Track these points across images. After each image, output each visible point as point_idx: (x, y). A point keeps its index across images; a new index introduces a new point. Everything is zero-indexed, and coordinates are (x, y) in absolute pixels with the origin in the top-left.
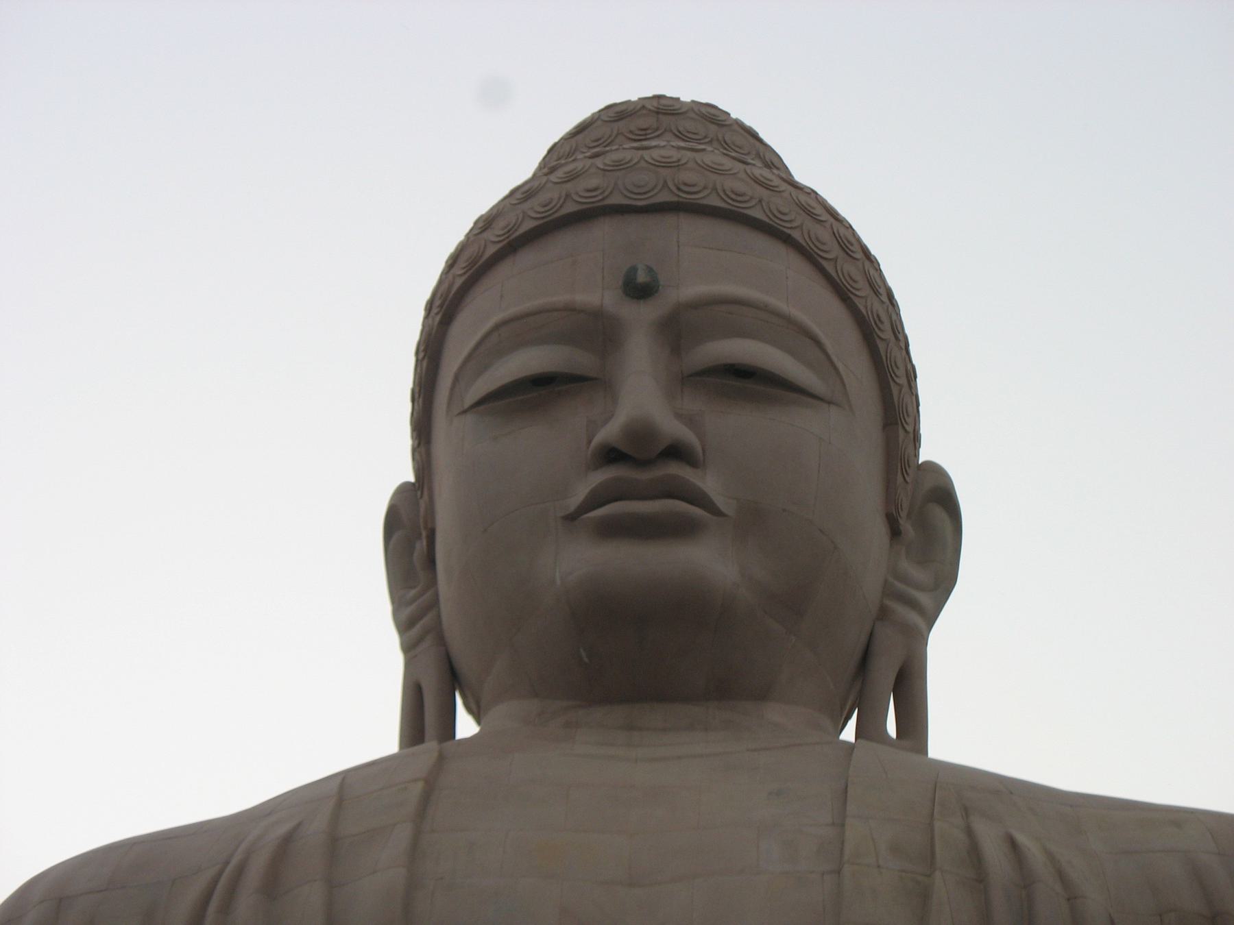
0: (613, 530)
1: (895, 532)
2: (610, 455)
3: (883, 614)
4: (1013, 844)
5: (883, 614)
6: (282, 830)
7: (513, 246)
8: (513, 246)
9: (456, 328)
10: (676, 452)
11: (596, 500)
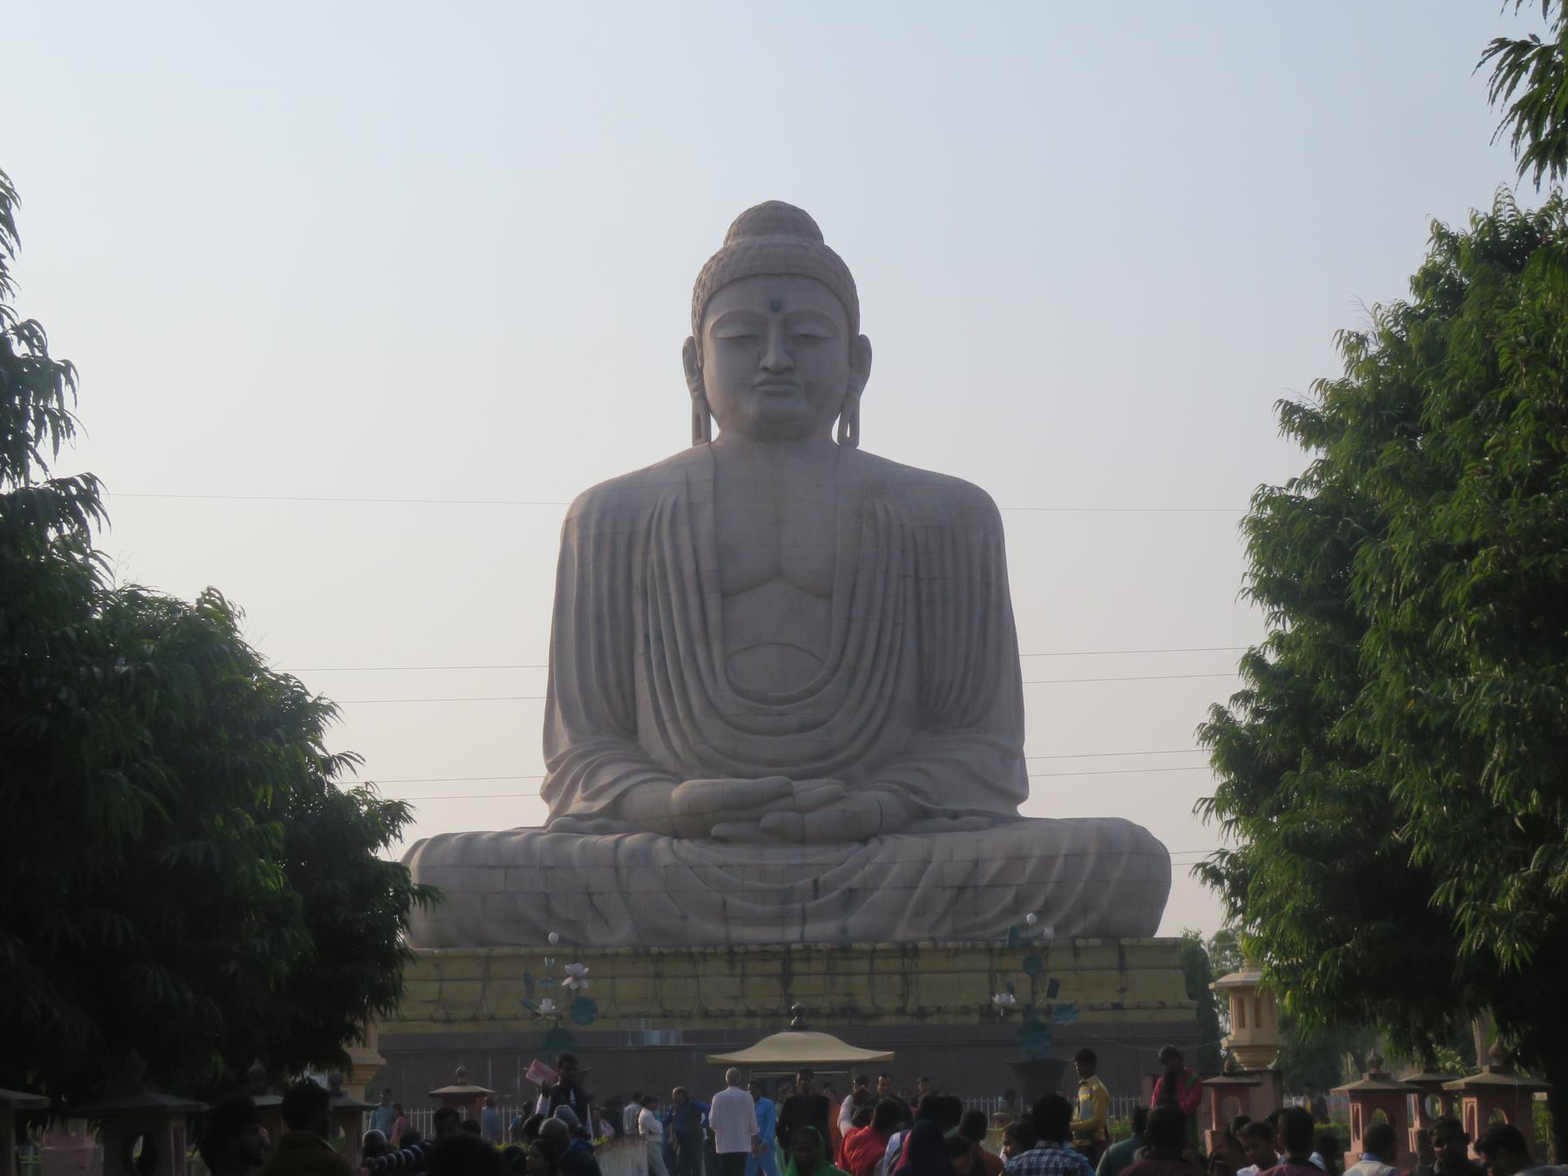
0: (767, 394)
1: (851, 365)
2: (766, 369)
3: (848, 395)
4: (887, 512)
5: (848, 395)
6: (671, 499)
7: (732, 282)
8: (732, 282)
9: (712, 305)
10: (789, 369)
11: (761, 384)
